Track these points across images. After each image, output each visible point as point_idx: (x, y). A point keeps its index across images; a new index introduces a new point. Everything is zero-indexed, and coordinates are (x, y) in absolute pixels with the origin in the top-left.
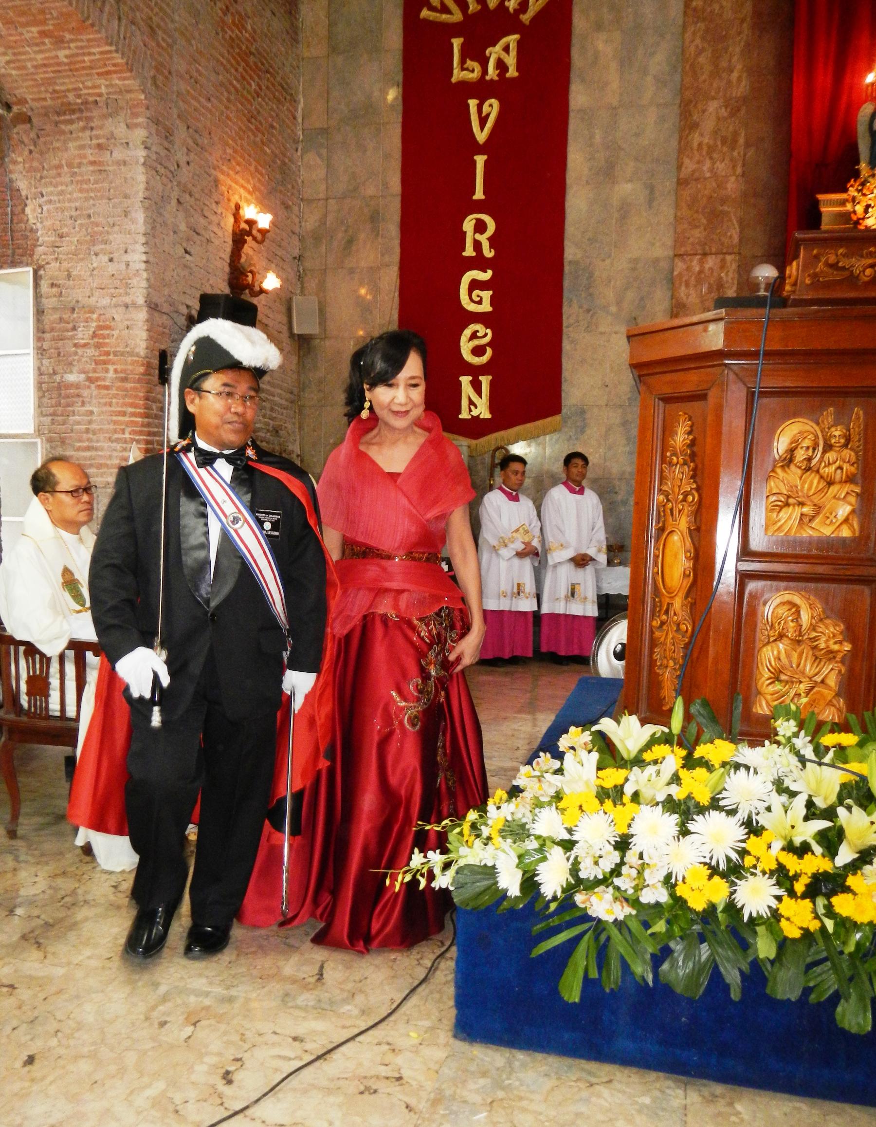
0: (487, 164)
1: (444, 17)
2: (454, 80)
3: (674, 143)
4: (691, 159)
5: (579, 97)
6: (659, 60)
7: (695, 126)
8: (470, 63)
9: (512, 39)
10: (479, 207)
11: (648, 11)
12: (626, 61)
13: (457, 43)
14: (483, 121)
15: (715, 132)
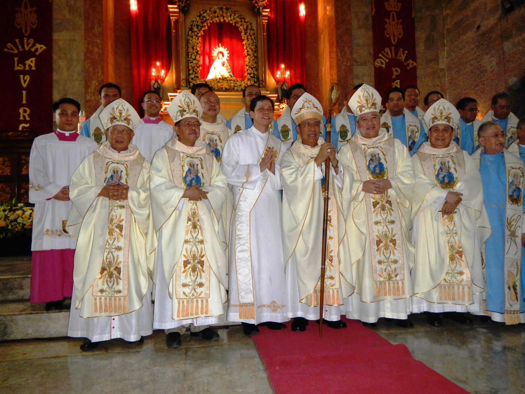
0: (26, 94)
1: (11, 51)
2: (15, 69)
3: (83, 90)
4: (88, 95)
5: (55, 77)
6: (78, 68)
7: (89, 87)
8: (20, 65)
9: (33, 59)
10: (24, 106)
11: (74, 55)
12: (68, 69)
13: (16, 59)
14: (25, 81)
15: (95, 89)
